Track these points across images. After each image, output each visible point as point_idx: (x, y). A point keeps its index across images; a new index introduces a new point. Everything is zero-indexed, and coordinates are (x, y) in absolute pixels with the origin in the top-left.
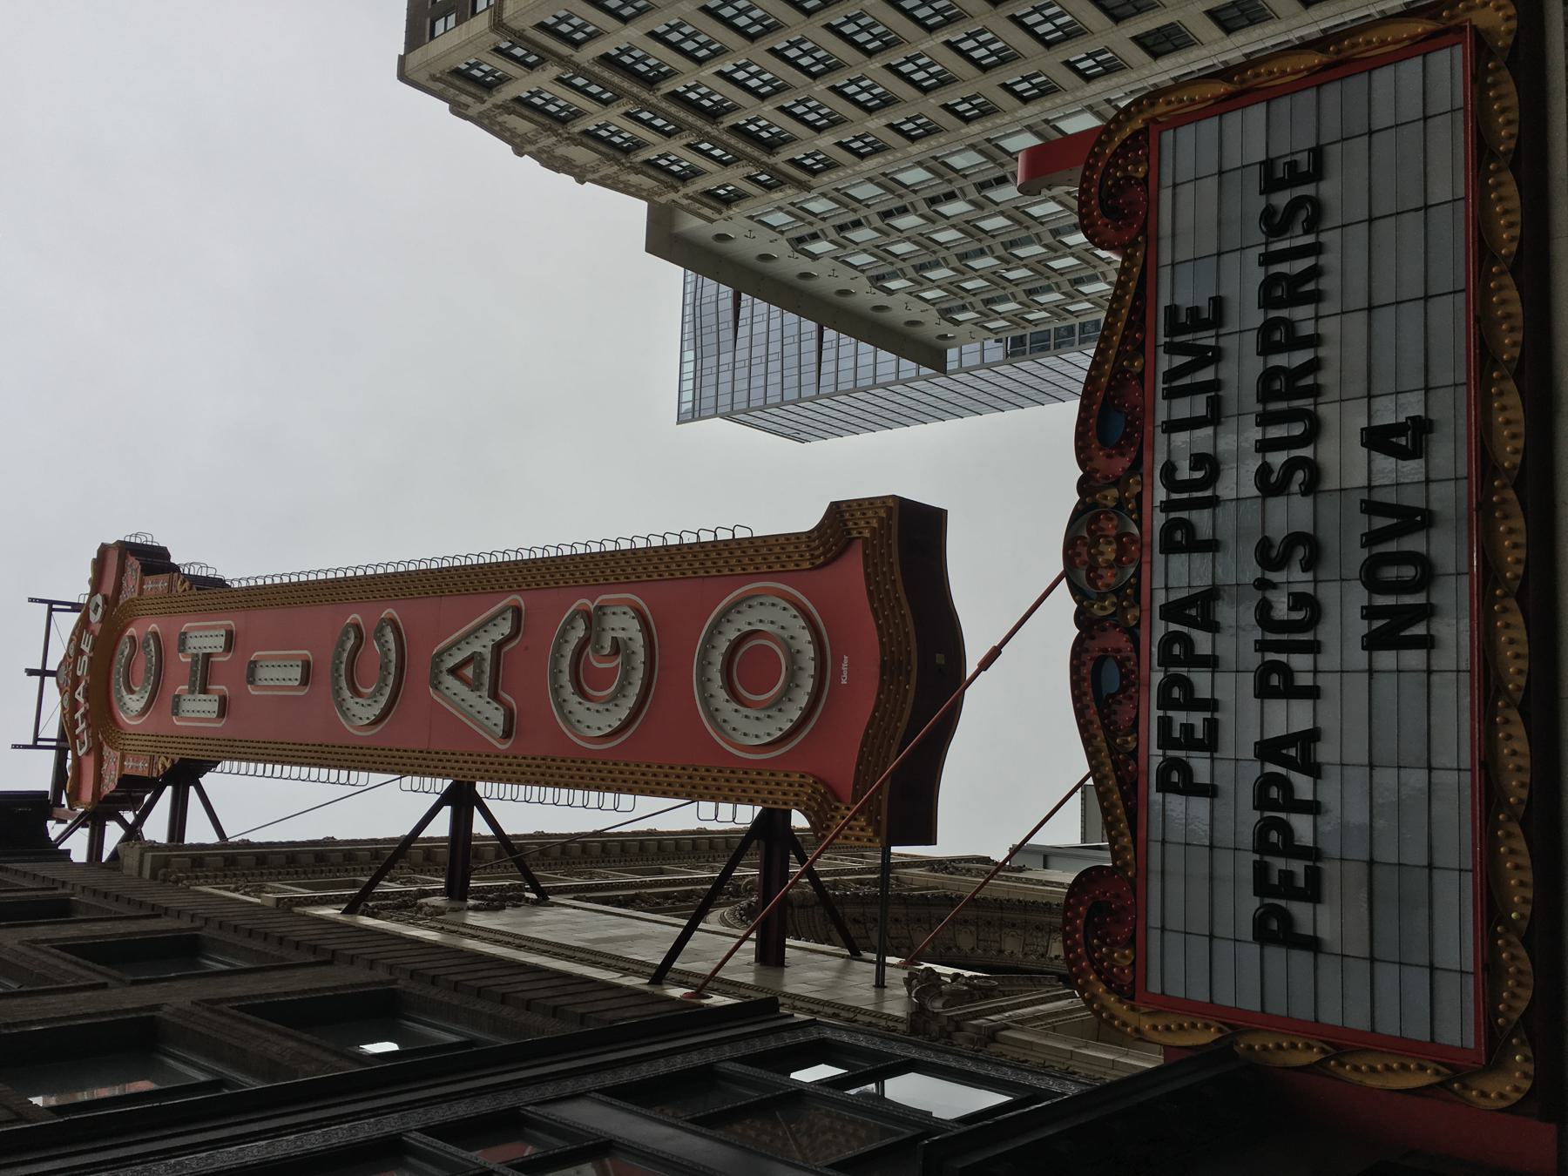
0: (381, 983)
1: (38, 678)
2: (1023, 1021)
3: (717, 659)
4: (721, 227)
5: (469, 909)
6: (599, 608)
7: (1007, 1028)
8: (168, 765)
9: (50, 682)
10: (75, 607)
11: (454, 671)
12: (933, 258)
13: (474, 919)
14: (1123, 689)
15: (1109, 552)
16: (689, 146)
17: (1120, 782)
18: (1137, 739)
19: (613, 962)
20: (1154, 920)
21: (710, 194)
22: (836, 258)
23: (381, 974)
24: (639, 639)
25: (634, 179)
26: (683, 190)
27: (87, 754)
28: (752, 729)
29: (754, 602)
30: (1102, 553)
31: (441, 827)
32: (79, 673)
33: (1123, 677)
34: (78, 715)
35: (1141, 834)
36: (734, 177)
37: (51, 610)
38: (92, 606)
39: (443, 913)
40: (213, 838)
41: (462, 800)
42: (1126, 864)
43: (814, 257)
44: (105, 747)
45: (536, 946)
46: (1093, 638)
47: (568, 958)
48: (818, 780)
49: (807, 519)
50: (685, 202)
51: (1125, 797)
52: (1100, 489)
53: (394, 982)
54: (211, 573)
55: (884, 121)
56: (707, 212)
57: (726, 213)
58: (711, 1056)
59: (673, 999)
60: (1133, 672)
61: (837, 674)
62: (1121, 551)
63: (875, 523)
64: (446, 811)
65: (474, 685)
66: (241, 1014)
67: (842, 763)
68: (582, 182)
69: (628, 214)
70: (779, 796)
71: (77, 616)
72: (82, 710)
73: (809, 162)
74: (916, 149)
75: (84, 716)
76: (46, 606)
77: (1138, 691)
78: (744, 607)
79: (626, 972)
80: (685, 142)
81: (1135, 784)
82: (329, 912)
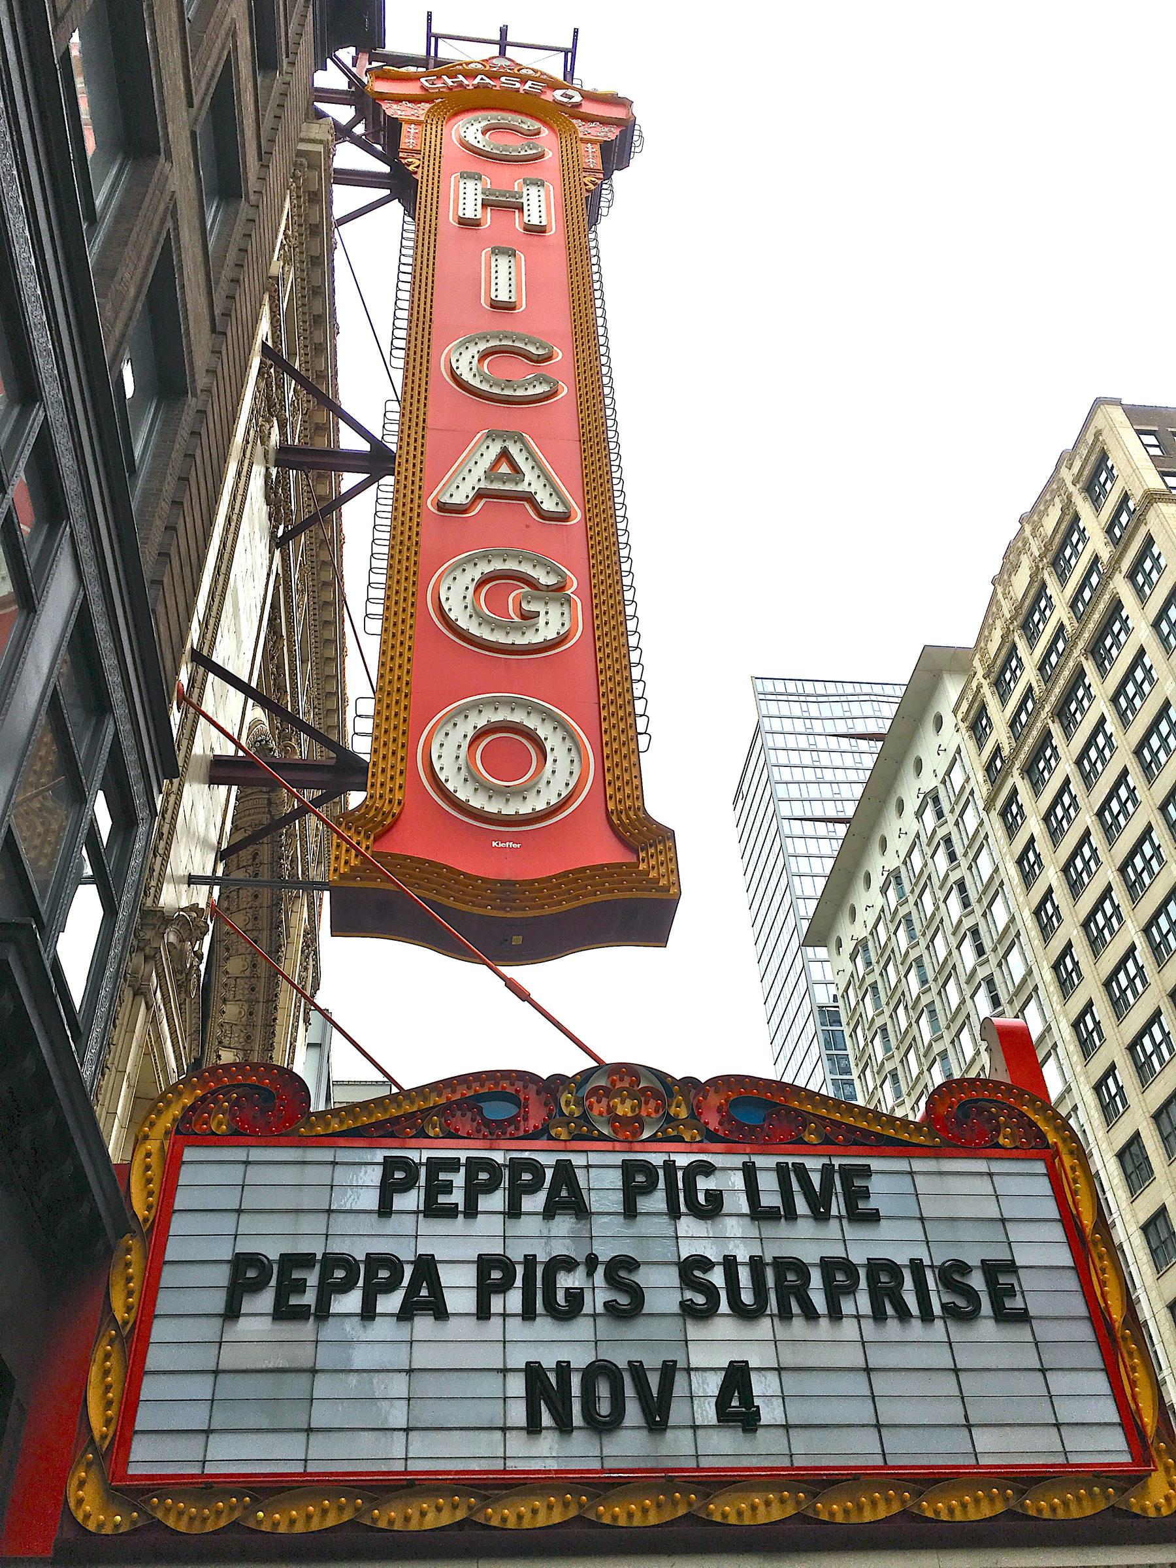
0: (193, 381)
1: (498, 38)
2: (154, 1021)
3: (518, 717)
4: (949, 721)
5: (267, 469)
6: (568, 600)
7: (148, 1008)
8: (410, 168)
9: (494, 50)
11: (505, 455)
12: (918, 934)
13: (258, 471)
14: (487, 1123)
15: (624, 1109)
16: (1030, 689)
17: (395, 1120)
18: (437, 1137)
19: (214, 614)
20: (257, 1154)
23: (202, 381)
24: (538, 639)
25: (997, 635)
26: (985, 683)
27: (423, 87)
28: (448, 751)
29: (574, 754)
30: (623, 1102)
31: (349, 441)
33: (499, 1123)
34: (461, 78)
35: (341, 1141)
36: (1000, 734)
38: (570, 92)
39: (263, 443)
40: (338, 212)
41: (377, 462)
42: (312, 1126)
43: (919, 814)
44: (428, 106)
45: (231, 536)
46: (538, 1093)
47: (218, 569)
48: (397, 819)
50: (974, 685)
51: (379, 1124)
52: (686, 1099)
53: (194, 395)
54: (604, 211)
56: (965, 706)
57: (962, 726)
58: (121, 711)
59: (177, 674)
60: (504, 1133)
61: (502, 837)
62: (624, 1121)
63: (653, 874)
64: (365, 446)
65: (491, 473)
66: (162, 241)
67: (410, 842)
69: (961, 632)
70: (380, 779)
71: (561, 77)
72: (466, 82)
73: (1014, 809)
74: (1027, 914)
75: (461, 84)
76: (569, 45)
77: (485, 1137)
78: (568, 744)
79: (205, 625)
80: (1034, 685)
81: (392, 1135)
82: (264, 328)
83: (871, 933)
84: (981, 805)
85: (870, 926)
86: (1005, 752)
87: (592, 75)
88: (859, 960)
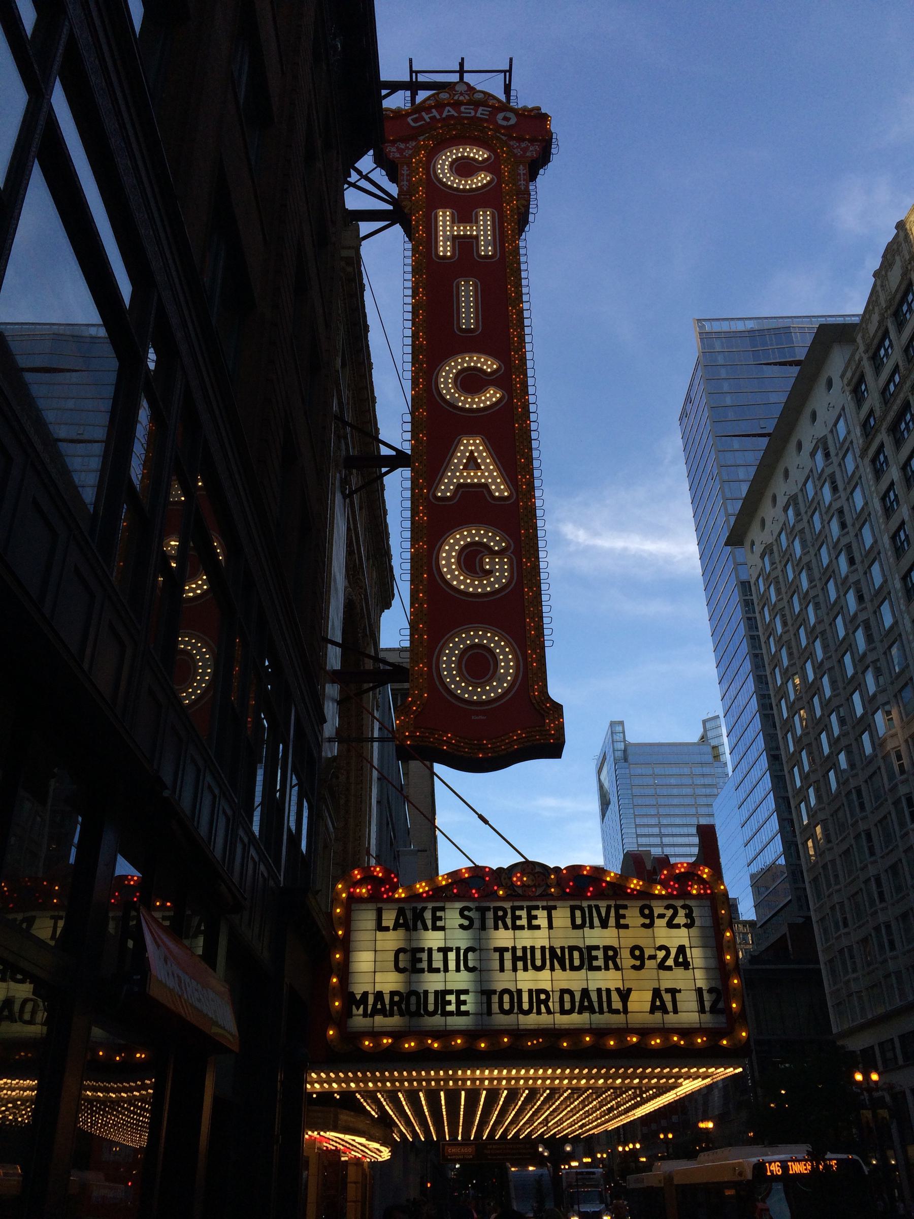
4: (837, 383)
10: (507, 89)
12: (809, 544)
16: (897, 366)
21: (862, 379)
22: (811, 471)
25: (876, 318)
26: (865, 357)
31: (385, 451)
32: (463, 108)
36: (873, 400)
37: (505, 72)
40: (362, 235)
41: (399, 460)
43: (813, 454)
49: (556, 691)
50: (857, 358)
55: (907, 519)
56: (849, 374)
57: (848, 389)
64: (394, 453)
68: (874, 276)
73: (882, 458)
74: (886, 540)
80: (900, 364)
83: (776, 540)
84: (858, 453)
85: (776, 534)
86: (878, 413)
87: (524, 99)
88: (766, 559)
